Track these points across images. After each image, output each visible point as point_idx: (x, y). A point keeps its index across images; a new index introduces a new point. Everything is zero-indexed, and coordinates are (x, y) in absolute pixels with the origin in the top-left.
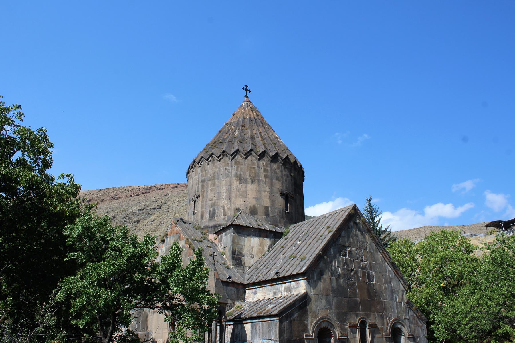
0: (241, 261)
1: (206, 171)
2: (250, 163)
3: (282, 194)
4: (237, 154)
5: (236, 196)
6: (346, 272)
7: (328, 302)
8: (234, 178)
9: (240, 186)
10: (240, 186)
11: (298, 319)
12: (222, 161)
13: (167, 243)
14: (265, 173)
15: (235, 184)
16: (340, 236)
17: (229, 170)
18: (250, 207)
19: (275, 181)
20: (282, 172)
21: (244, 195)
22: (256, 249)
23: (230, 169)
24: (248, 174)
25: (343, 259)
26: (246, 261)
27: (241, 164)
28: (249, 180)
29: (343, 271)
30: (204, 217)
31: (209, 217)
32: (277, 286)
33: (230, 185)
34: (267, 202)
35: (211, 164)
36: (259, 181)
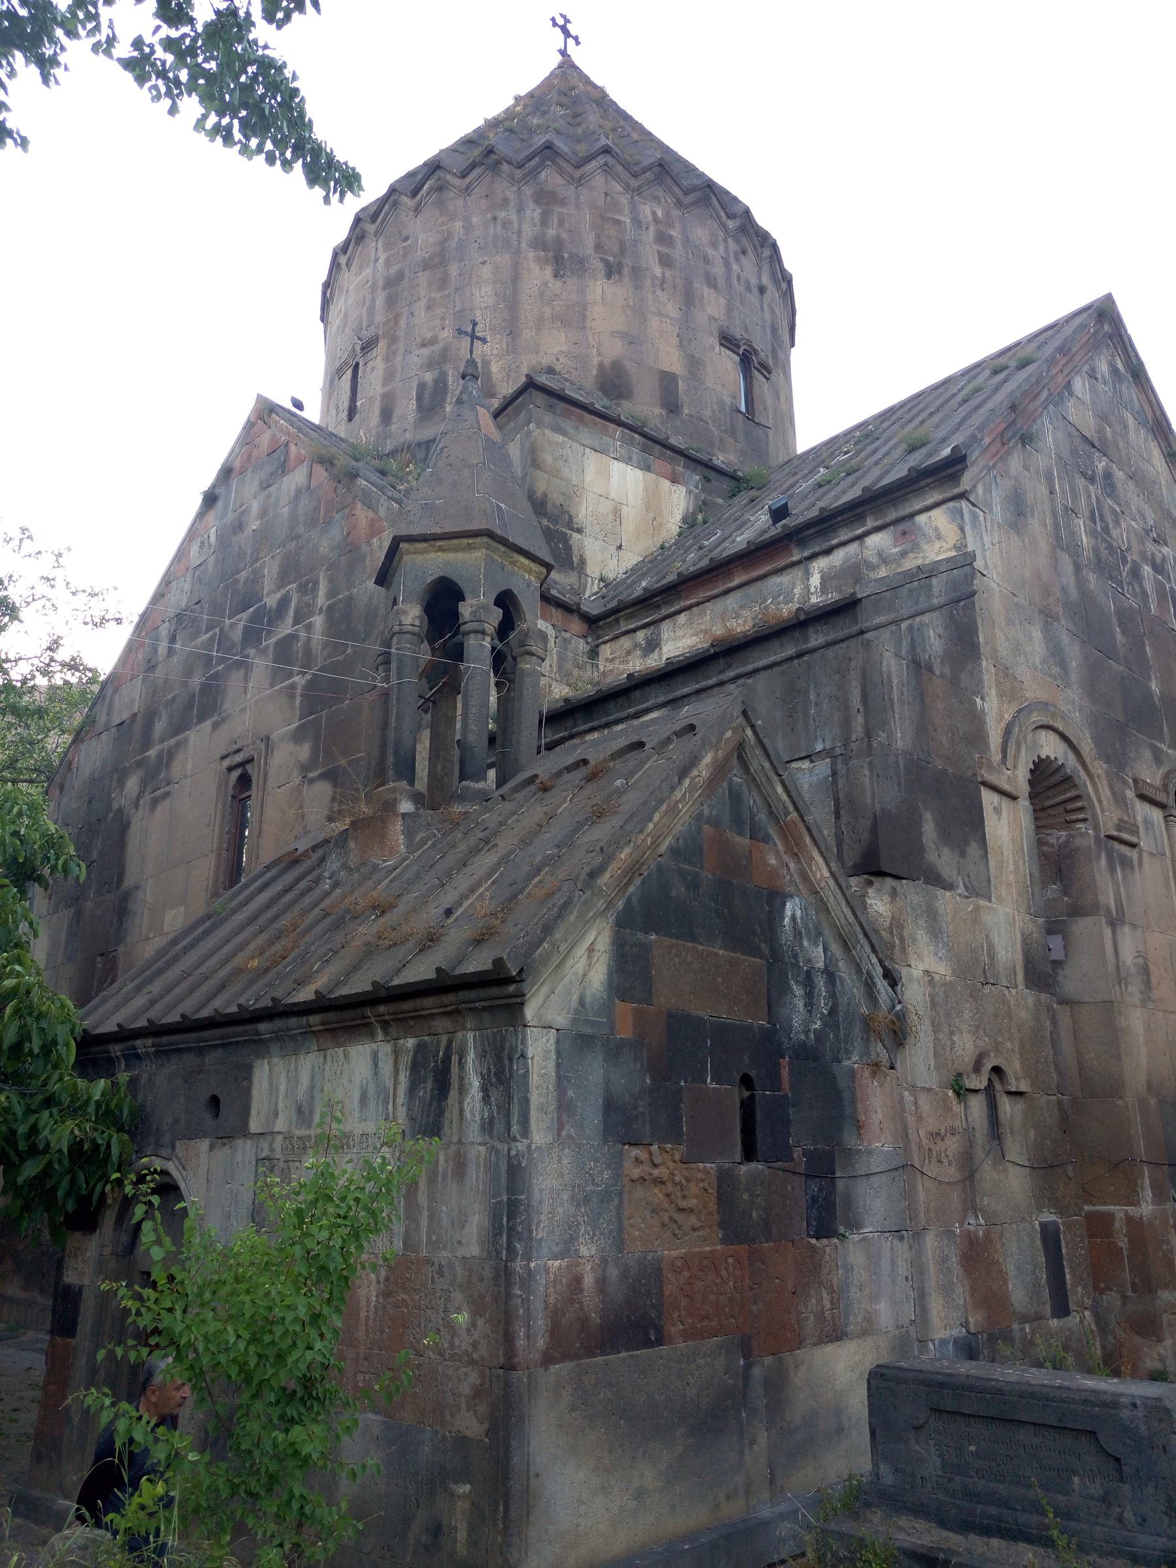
0: (568, 548)
1: (406, 239)
2: (601, 202)
3: (727, 341)
4: (542, 165)
5: (540, 323)
6: (1105, 553)
7: (1056, 653)
8: (531, 254)
9: (558, 284)
10: (556, 286)
11: (947, 671)
12: (479, 191)
13: (226, 507)
14: (663, 249)
15: (537, 275)
16: (1068, 386)
17: (506, 224)
18: (601, 365)
19: (706, 291)
20: (726, 261)
21: (575, 318)
22: (632, 513)
23: (514, 218)
24: (589, 240)
25: (1089, 496)
26: (588, 555)
27: (563, 202)
28: (597, 264)
29: (1093, 542)
30: (397, 413)
31: (420, 407)
32: (777, 579)
33: (516, 279)
34: (671, 360)
35: (428, 213)
36: (637, 273)
